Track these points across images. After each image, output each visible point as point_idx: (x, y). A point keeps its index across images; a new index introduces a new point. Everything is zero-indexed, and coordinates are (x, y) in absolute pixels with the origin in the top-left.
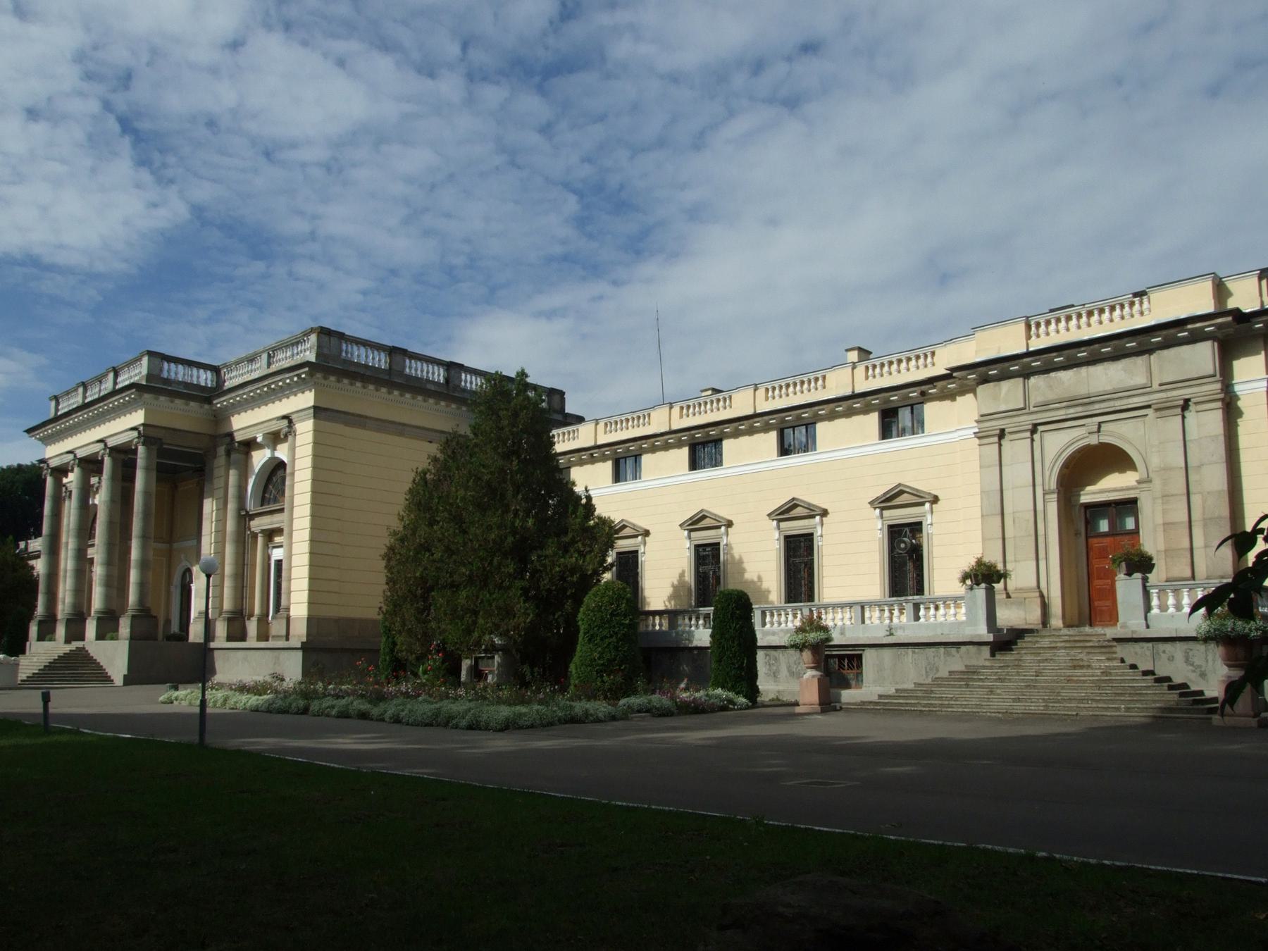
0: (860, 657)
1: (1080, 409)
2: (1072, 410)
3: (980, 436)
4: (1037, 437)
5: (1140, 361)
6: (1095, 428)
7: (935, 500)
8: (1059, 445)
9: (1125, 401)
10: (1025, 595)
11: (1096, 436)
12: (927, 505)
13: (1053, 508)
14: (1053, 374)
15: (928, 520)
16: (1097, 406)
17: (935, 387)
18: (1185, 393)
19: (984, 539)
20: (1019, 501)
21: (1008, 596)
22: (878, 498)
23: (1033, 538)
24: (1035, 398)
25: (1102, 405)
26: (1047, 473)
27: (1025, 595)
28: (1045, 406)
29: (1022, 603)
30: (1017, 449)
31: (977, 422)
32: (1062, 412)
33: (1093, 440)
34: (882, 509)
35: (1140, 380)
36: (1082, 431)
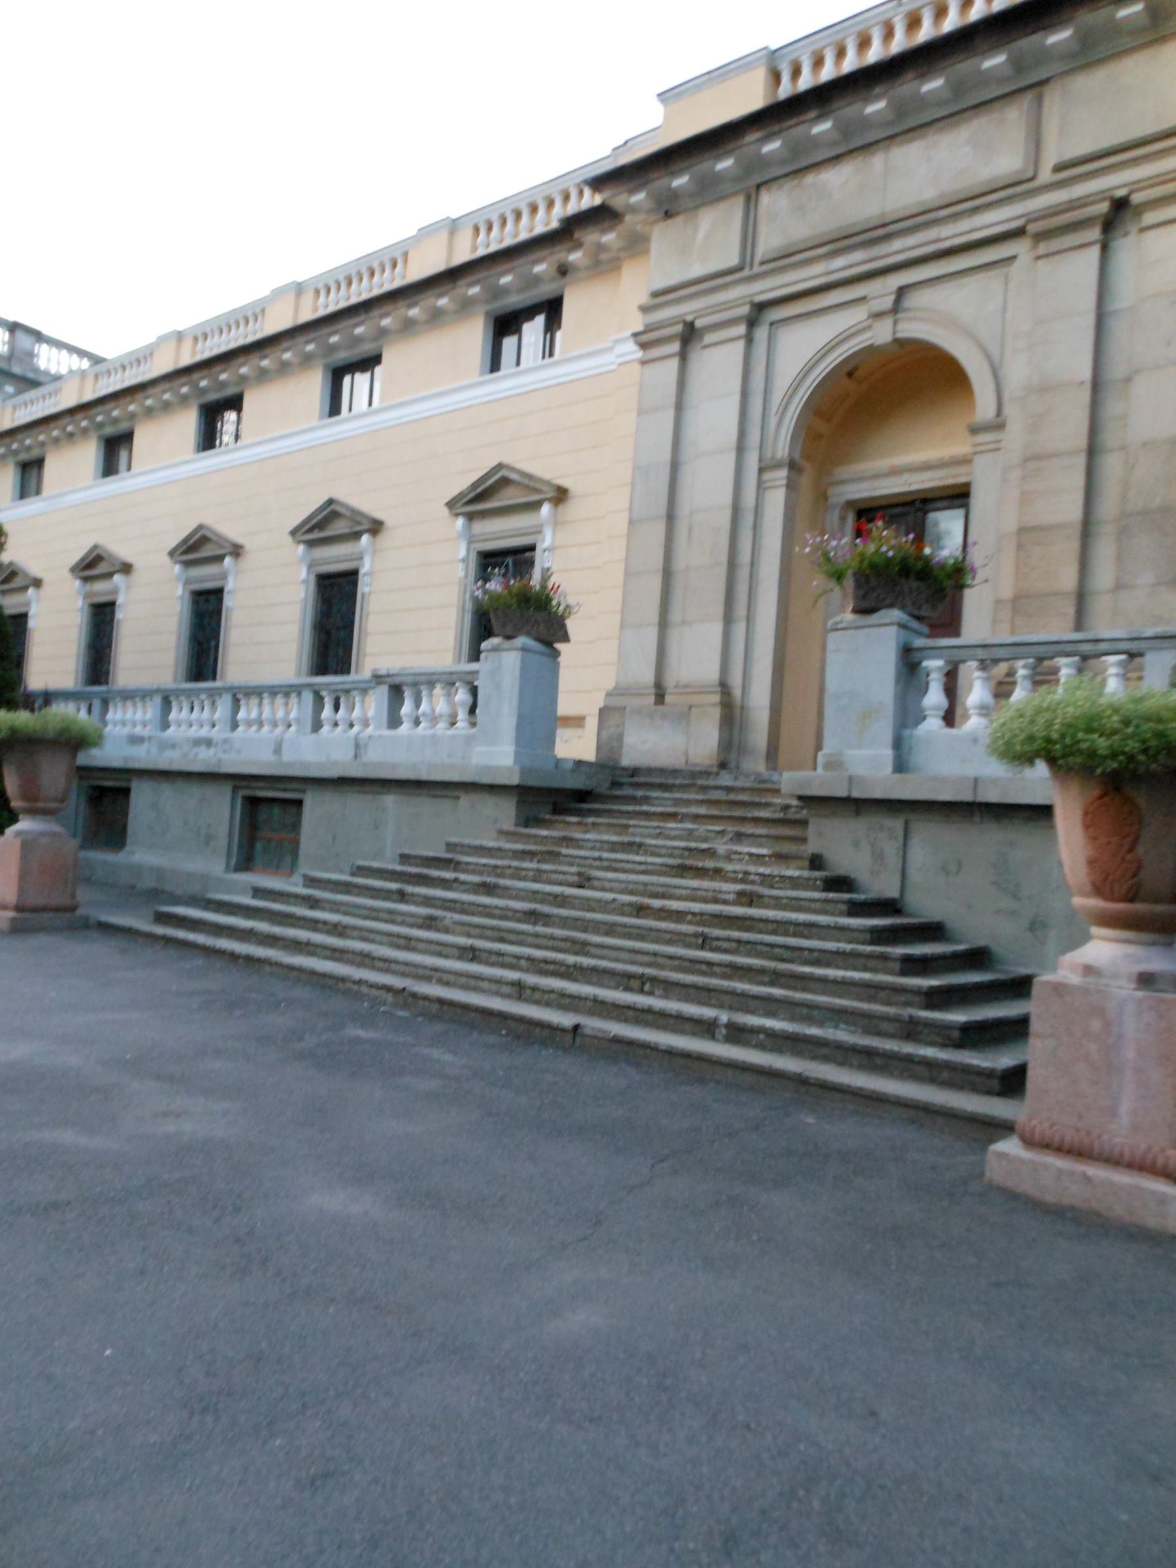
0: (299, 803)
1: (858, 256)
2: (840, 262)
3: (646, 341)
4: (761, 333)
5: (1014, 116)
6: (888, 302)
7: (561, 495)
8: (806, 349)
9: (964, 225)
10: (696, 699)
11: (888, 322)
12: (546, 509)
13: (776, 501)
14: (809, 178)
15: (546, 540)
16: (897, 244)
17: (579, 245)
18: (1116, 182)
19: (628, 574)
20: (710, 485)
21: (660, 698)
22: (461, 495)
23: (722, 571)
24: (769, 241)
25: (910, 241)
26: (773, 421)
27: (696, 699)
28: (785, 259)
29: (684, 716)
30: (719, 364)
31: (644, 309)
32: (818, 268)
33: (882, 334)
34: (471, 517)
35: (1007, 161)
36: (858, 315)
